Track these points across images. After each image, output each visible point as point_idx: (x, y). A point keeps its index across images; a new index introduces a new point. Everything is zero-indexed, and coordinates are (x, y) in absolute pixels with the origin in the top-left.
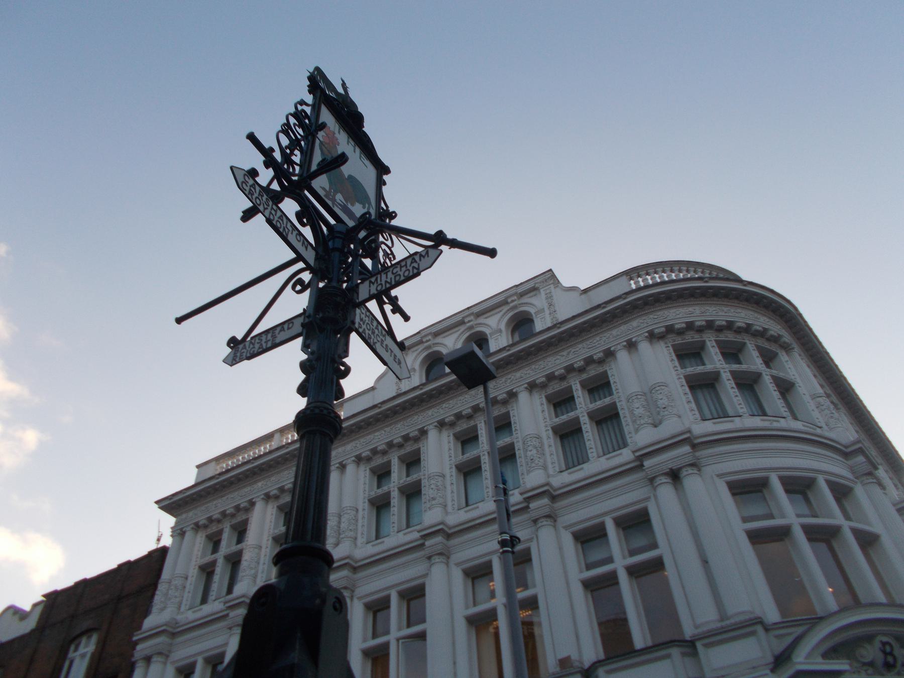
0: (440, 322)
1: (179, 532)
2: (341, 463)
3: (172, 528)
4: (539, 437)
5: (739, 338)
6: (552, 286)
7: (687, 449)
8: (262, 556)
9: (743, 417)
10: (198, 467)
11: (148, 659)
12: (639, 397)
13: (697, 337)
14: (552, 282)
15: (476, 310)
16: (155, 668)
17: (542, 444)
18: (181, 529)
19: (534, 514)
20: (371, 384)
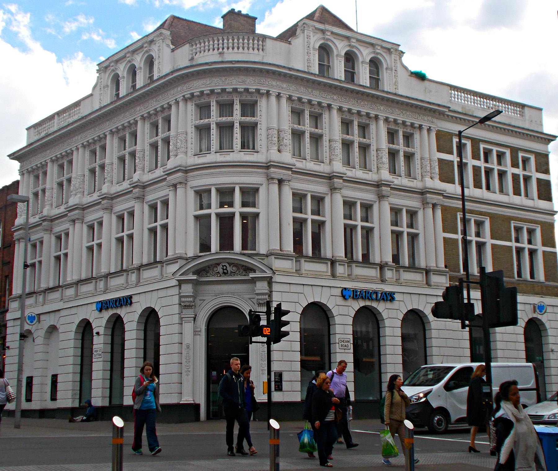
0: (116, 53)
1: (22, 173)
2: (76, 146)
3: (19, 170)
4: (143, 151)
5: (230, 98)
6: (161, 41)
7: (180, 174)
8: (54, 194)
9: (211, 154)
10: (28, 129)
11: (19, 240)
12: (173, 138)
13: (207, 100)
14: (161, 38)
15: (131, 49)
16: (22, 245)
17: (144, 155)
18: (22, 172)
19: (134, 196)
20: (89, 92)
